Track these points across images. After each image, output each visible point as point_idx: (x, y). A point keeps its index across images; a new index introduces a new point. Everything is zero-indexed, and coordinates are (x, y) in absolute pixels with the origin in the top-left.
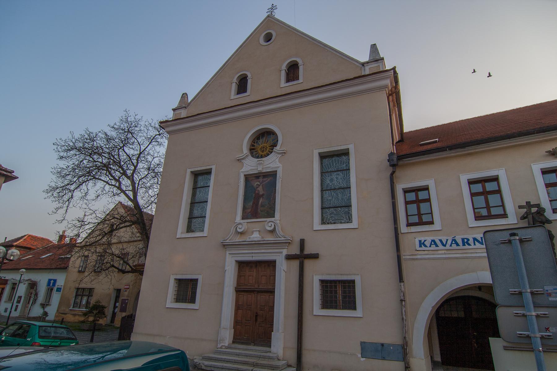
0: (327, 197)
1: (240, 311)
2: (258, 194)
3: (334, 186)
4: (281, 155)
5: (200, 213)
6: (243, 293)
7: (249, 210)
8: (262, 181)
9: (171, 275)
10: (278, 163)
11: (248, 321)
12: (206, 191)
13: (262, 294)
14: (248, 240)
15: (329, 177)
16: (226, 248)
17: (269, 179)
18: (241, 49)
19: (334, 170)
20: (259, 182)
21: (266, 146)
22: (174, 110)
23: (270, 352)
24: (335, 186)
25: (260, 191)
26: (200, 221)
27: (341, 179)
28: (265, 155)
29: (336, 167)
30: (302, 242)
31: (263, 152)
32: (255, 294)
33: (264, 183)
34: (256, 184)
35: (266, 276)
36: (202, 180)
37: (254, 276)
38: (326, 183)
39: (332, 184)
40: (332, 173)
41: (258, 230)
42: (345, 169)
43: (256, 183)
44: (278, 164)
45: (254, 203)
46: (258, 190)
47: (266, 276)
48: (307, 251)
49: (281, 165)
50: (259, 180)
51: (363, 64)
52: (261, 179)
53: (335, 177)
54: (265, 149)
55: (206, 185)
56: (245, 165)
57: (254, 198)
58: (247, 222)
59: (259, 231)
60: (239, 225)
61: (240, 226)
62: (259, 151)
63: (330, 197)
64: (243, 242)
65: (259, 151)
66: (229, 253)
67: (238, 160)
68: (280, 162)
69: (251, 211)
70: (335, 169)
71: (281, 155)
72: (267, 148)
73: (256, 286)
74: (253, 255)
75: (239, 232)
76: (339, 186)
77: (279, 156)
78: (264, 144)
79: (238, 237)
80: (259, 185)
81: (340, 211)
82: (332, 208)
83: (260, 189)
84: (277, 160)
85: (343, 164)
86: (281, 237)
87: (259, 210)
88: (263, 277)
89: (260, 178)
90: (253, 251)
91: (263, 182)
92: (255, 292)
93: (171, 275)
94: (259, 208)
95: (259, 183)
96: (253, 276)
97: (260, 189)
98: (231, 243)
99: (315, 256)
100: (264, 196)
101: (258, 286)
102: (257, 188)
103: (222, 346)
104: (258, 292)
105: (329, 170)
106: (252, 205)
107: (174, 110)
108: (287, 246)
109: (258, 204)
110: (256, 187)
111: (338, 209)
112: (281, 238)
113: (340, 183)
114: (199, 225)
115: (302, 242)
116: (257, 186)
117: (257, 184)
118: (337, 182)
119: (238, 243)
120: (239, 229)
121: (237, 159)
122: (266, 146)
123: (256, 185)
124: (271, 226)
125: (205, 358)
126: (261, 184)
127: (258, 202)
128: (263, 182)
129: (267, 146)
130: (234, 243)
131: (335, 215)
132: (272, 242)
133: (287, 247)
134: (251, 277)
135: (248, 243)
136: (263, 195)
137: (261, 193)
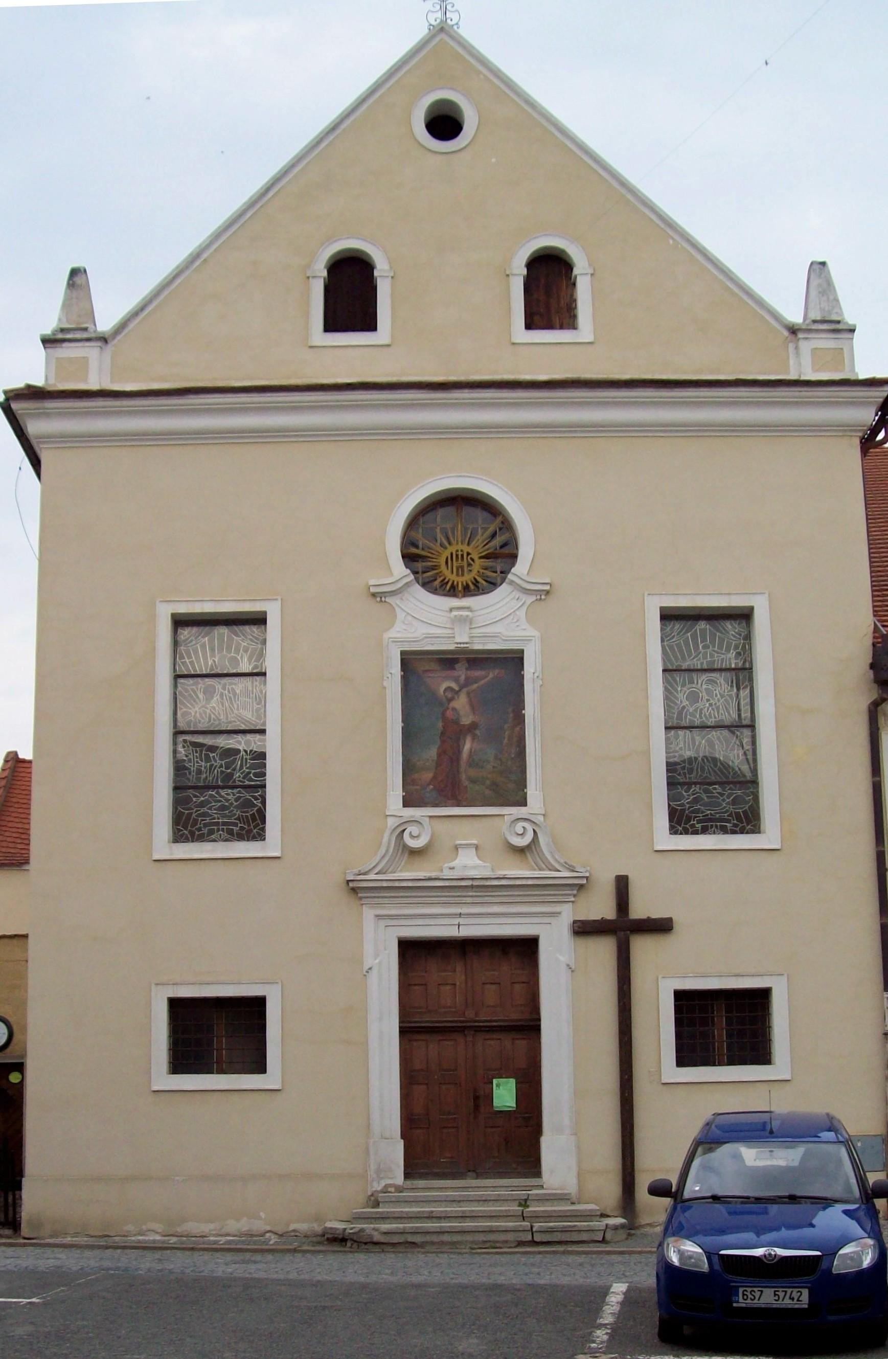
0: (681, 749)
1: (419, 1091)
2: (456, 722)
3: (700, 716)
4: (534, 598)
5: (222, 772)
6: (423, 1037)
7: (429, 775)
8: (467, 679)
9: (153, 986)
10: (525, 625)
11: (449, 1113)
12: (235, 694)
13: (487, 1037)
14: (447, 874)
15: (683, 685)
16: (361, 898)
17: (491, 676)
18: (331, 137)
19: (699, 667)
20: (456, 680)
21: (468, 554)
22: (48, 342)
23: (542, 1187)
24: (705, 715)
25: (462, 713)
26: (227, 800)
27: (722, 696)
28: (468, 585)
29: (705, 657)
30: (622, 885)
31: (457, 575)
32: (465, 1036)
33: (475, 686)
34: (444, 685)
35: (499, 984)
36: (212, 650)
37: (458, 984)
38: (676, 704)
39: (696, 710)
40: (694, 675)
41: (475, 842)
42: (733, 666)
43: (443, 684)
44: (524, 629)
45: (441, 753)
46: (454, 709)
47: (499, 984)
48: (639, 910)
49: (536, 633)
50: (455, 673)
51: (793, 330)
52: (461, 672)
53: (704, 687)
54: (465, 564)
55: (234, 671)
56: (400, 615)
57: (443, 734)
58: (430, 817)
59: (477, 847)
60: (411, 824)
61: (413, 829)
62: (443, 567)
63: (689, 750)
64: (430, 879)
65: (443, 567)
66: (378, 917)
67: (374, 595)
68: (530, 619)
69: (435, 777)
70: (701, 664)
71: (534, 598)
72: (473, 560)
73: (470, 1014)
74: (462, 921)
75: (405, 846)
76: (715, 717)
77: (529, 602)
78: (460, 547)
79: (403, 864)
80: (457, 693)
81: (722, 795)
82: (695, 784)
83: (461, 703)
84: (522, 613)
85: (728, 650)
86: (559, 868)
87: (463, 776)
88: (488, 986)
89: (457, 666)
90: (464, 910)
91: (468, 682)
92: (466, 1032)
93: (153, 986)
94: (462, 769)
95: (454, 685)
96: (455, 985)
97: (461, 703)
98: (385, 884)
99: (662, 927)
100: (478, 732)
101: (476, 1014)
102: (450, 700)
103: (386, 1186)
104: (478, 1030)
105: (685, 666)
106: (435, 758)
107: (48, 342)
108: (575, 896)
109: (458, 759)
110: (444, 700)
111: (715, 789)
112: (560, 871)
113: (718, 708)
114: (224, 816)
115: (622, 885)
116: (449, 695)
117: (449, 689)
118: (711, 705)
119: (410, 884)
120: (412, 837)
121: (373, 590)
122: (468, 554)
123: (446, 690)
124: (522, 834)
125: (358, 1218)
126: (465, 690)
127: (459, 752)
128: (468, 682)
129: (475, 556)
130: (397, 884)
131: (705, 805)
132: (530, 882)
133: (573, 899)
134: (448, 987)
135: (447, 884)
136: (473, 727)
137: (466, 720)
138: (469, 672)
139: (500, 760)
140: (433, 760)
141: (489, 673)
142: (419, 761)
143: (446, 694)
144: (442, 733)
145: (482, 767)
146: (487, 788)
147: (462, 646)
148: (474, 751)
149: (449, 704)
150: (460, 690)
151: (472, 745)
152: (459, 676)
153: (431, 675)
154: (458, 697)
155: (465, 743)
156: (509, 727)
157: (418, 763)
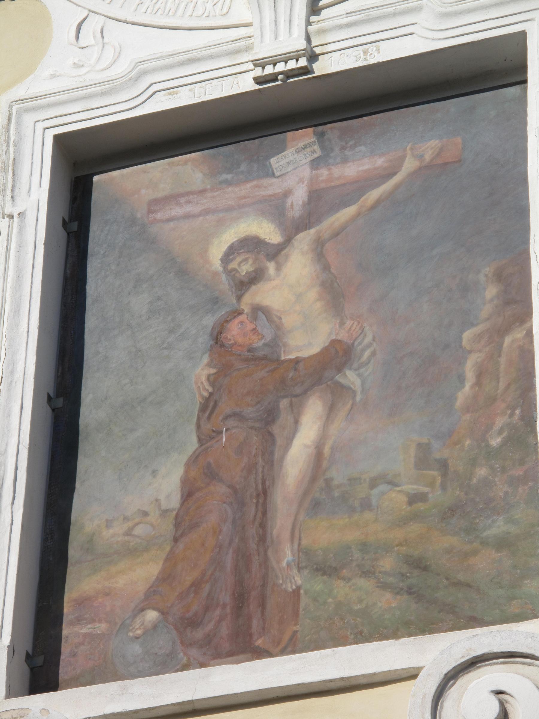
25: (288, 321)
106: (175, 502)
110: (224, 281)
123: (227, 258)
138: (324, 173)
139: (443, 466)
140: (165, 513)
141: (402, 159)
142: (109, 524)
143: (233, 265)
144: (203, 408)
145: (366, 505)
146: (384, 586)
147: (281, 67)
148: (333, 449)
149: (239, 298)
150: (288, 241)
151: (325, 427)
152: (287, 193)
153: (177, 211)
154: (278, 268)
155: (297, 422)
156: (480, 336)
157: (107, 533)
